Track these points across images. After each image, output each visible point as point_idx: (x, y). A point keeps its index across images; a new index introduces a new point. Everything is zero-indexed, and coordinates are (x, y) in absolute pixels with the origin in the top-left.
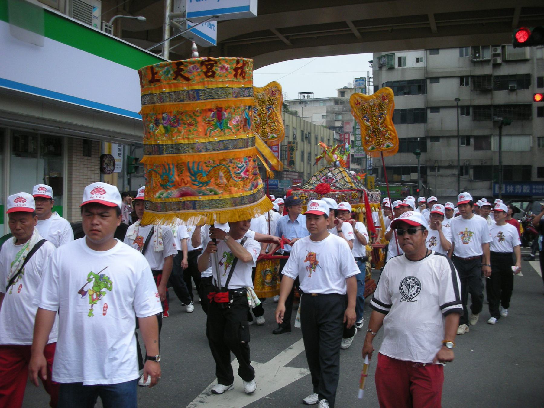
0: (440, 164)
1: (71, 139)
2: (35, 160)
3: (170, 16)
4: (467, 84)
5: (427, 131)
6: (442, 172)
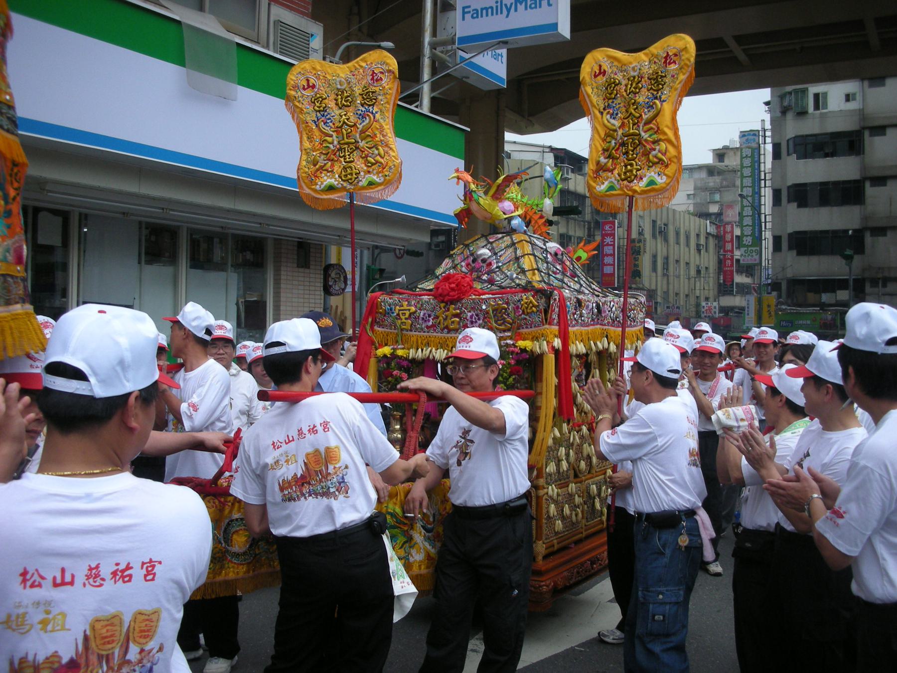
0: (886, 274)
1: (278, 242)
2: (222, 274)
3: (430, 44)
5: (865, 218)
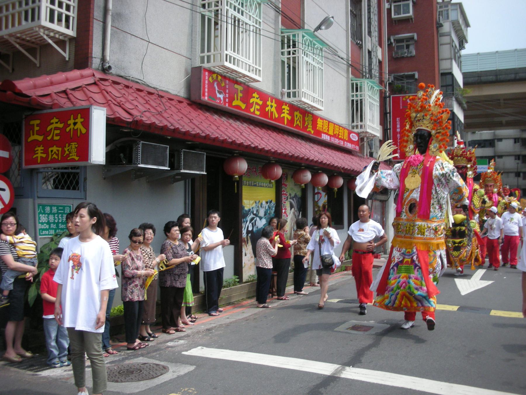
4: (518, 142)
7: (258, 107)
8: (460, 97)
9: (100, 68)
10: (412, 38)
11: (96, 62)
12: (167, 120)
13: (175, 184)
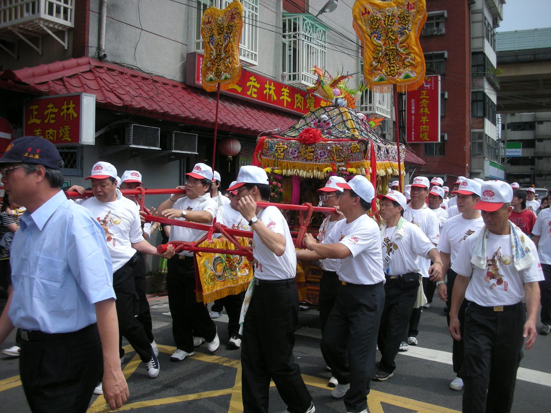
0: (542, 172)
6: (544, 178)
7: (255, 90)
8: (492, 78)
9: (96, 57)
10: (442, 16)
11: (92, 51)
12: (157, 104)
13: (170, 163)
